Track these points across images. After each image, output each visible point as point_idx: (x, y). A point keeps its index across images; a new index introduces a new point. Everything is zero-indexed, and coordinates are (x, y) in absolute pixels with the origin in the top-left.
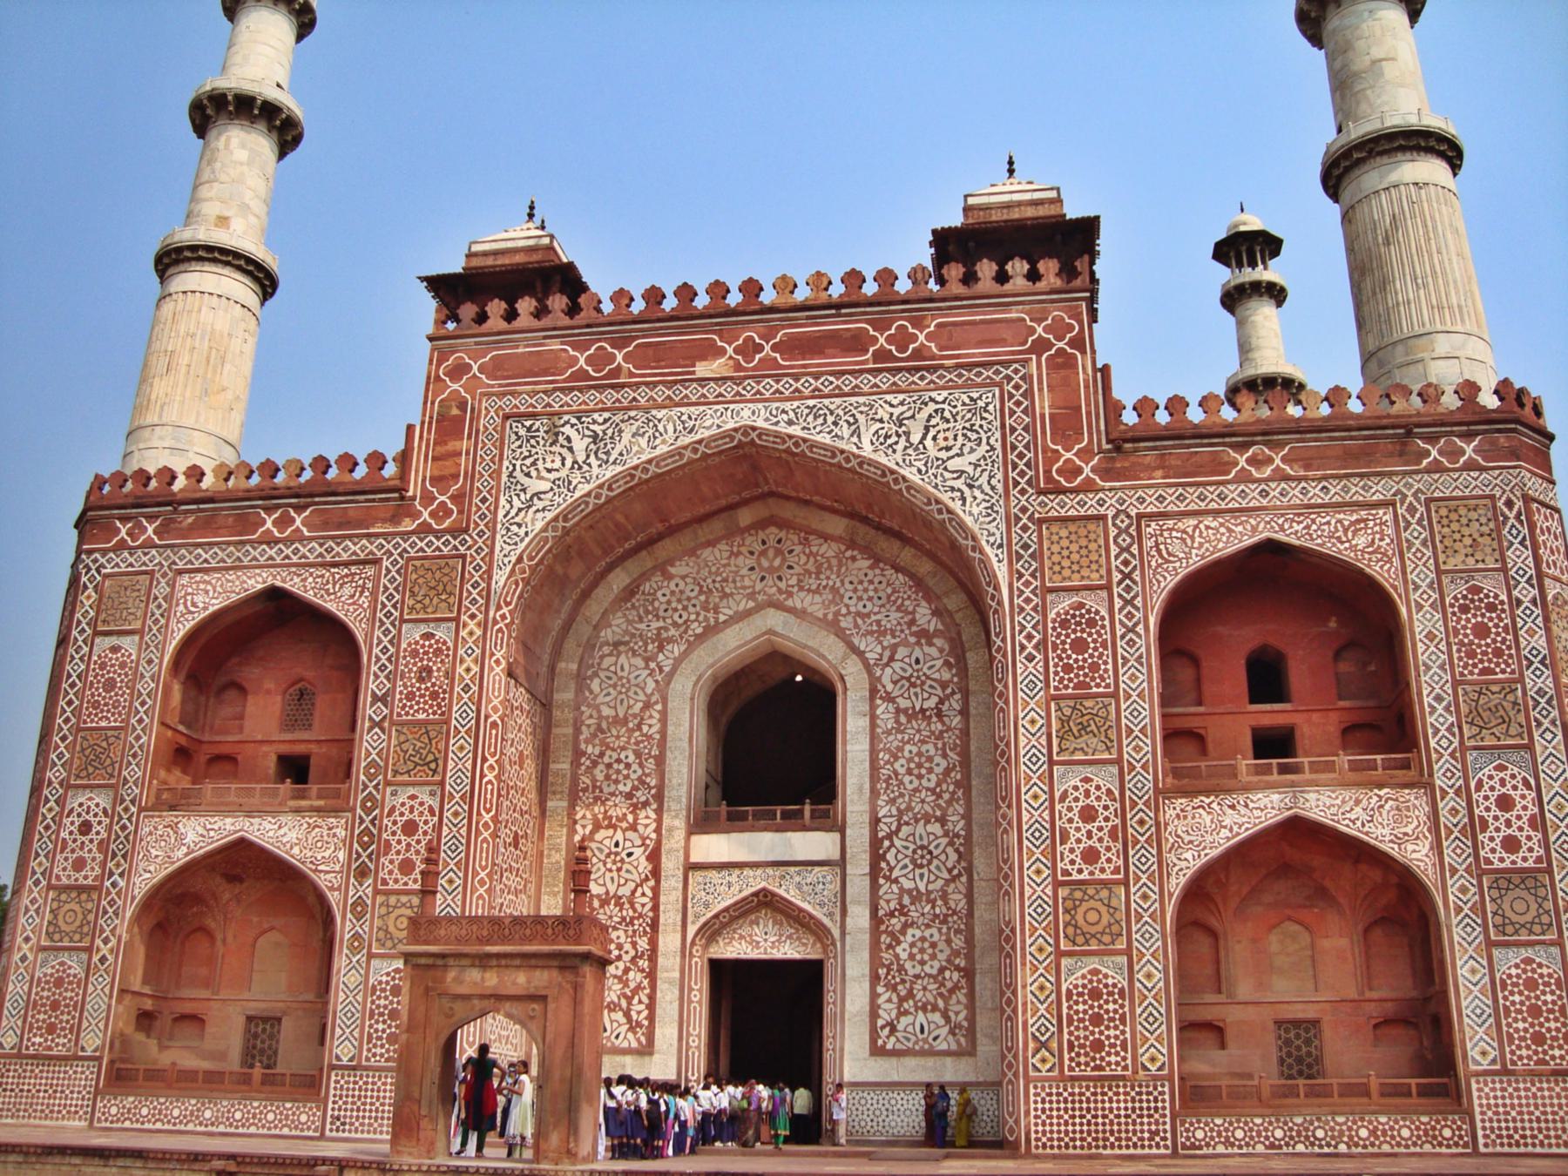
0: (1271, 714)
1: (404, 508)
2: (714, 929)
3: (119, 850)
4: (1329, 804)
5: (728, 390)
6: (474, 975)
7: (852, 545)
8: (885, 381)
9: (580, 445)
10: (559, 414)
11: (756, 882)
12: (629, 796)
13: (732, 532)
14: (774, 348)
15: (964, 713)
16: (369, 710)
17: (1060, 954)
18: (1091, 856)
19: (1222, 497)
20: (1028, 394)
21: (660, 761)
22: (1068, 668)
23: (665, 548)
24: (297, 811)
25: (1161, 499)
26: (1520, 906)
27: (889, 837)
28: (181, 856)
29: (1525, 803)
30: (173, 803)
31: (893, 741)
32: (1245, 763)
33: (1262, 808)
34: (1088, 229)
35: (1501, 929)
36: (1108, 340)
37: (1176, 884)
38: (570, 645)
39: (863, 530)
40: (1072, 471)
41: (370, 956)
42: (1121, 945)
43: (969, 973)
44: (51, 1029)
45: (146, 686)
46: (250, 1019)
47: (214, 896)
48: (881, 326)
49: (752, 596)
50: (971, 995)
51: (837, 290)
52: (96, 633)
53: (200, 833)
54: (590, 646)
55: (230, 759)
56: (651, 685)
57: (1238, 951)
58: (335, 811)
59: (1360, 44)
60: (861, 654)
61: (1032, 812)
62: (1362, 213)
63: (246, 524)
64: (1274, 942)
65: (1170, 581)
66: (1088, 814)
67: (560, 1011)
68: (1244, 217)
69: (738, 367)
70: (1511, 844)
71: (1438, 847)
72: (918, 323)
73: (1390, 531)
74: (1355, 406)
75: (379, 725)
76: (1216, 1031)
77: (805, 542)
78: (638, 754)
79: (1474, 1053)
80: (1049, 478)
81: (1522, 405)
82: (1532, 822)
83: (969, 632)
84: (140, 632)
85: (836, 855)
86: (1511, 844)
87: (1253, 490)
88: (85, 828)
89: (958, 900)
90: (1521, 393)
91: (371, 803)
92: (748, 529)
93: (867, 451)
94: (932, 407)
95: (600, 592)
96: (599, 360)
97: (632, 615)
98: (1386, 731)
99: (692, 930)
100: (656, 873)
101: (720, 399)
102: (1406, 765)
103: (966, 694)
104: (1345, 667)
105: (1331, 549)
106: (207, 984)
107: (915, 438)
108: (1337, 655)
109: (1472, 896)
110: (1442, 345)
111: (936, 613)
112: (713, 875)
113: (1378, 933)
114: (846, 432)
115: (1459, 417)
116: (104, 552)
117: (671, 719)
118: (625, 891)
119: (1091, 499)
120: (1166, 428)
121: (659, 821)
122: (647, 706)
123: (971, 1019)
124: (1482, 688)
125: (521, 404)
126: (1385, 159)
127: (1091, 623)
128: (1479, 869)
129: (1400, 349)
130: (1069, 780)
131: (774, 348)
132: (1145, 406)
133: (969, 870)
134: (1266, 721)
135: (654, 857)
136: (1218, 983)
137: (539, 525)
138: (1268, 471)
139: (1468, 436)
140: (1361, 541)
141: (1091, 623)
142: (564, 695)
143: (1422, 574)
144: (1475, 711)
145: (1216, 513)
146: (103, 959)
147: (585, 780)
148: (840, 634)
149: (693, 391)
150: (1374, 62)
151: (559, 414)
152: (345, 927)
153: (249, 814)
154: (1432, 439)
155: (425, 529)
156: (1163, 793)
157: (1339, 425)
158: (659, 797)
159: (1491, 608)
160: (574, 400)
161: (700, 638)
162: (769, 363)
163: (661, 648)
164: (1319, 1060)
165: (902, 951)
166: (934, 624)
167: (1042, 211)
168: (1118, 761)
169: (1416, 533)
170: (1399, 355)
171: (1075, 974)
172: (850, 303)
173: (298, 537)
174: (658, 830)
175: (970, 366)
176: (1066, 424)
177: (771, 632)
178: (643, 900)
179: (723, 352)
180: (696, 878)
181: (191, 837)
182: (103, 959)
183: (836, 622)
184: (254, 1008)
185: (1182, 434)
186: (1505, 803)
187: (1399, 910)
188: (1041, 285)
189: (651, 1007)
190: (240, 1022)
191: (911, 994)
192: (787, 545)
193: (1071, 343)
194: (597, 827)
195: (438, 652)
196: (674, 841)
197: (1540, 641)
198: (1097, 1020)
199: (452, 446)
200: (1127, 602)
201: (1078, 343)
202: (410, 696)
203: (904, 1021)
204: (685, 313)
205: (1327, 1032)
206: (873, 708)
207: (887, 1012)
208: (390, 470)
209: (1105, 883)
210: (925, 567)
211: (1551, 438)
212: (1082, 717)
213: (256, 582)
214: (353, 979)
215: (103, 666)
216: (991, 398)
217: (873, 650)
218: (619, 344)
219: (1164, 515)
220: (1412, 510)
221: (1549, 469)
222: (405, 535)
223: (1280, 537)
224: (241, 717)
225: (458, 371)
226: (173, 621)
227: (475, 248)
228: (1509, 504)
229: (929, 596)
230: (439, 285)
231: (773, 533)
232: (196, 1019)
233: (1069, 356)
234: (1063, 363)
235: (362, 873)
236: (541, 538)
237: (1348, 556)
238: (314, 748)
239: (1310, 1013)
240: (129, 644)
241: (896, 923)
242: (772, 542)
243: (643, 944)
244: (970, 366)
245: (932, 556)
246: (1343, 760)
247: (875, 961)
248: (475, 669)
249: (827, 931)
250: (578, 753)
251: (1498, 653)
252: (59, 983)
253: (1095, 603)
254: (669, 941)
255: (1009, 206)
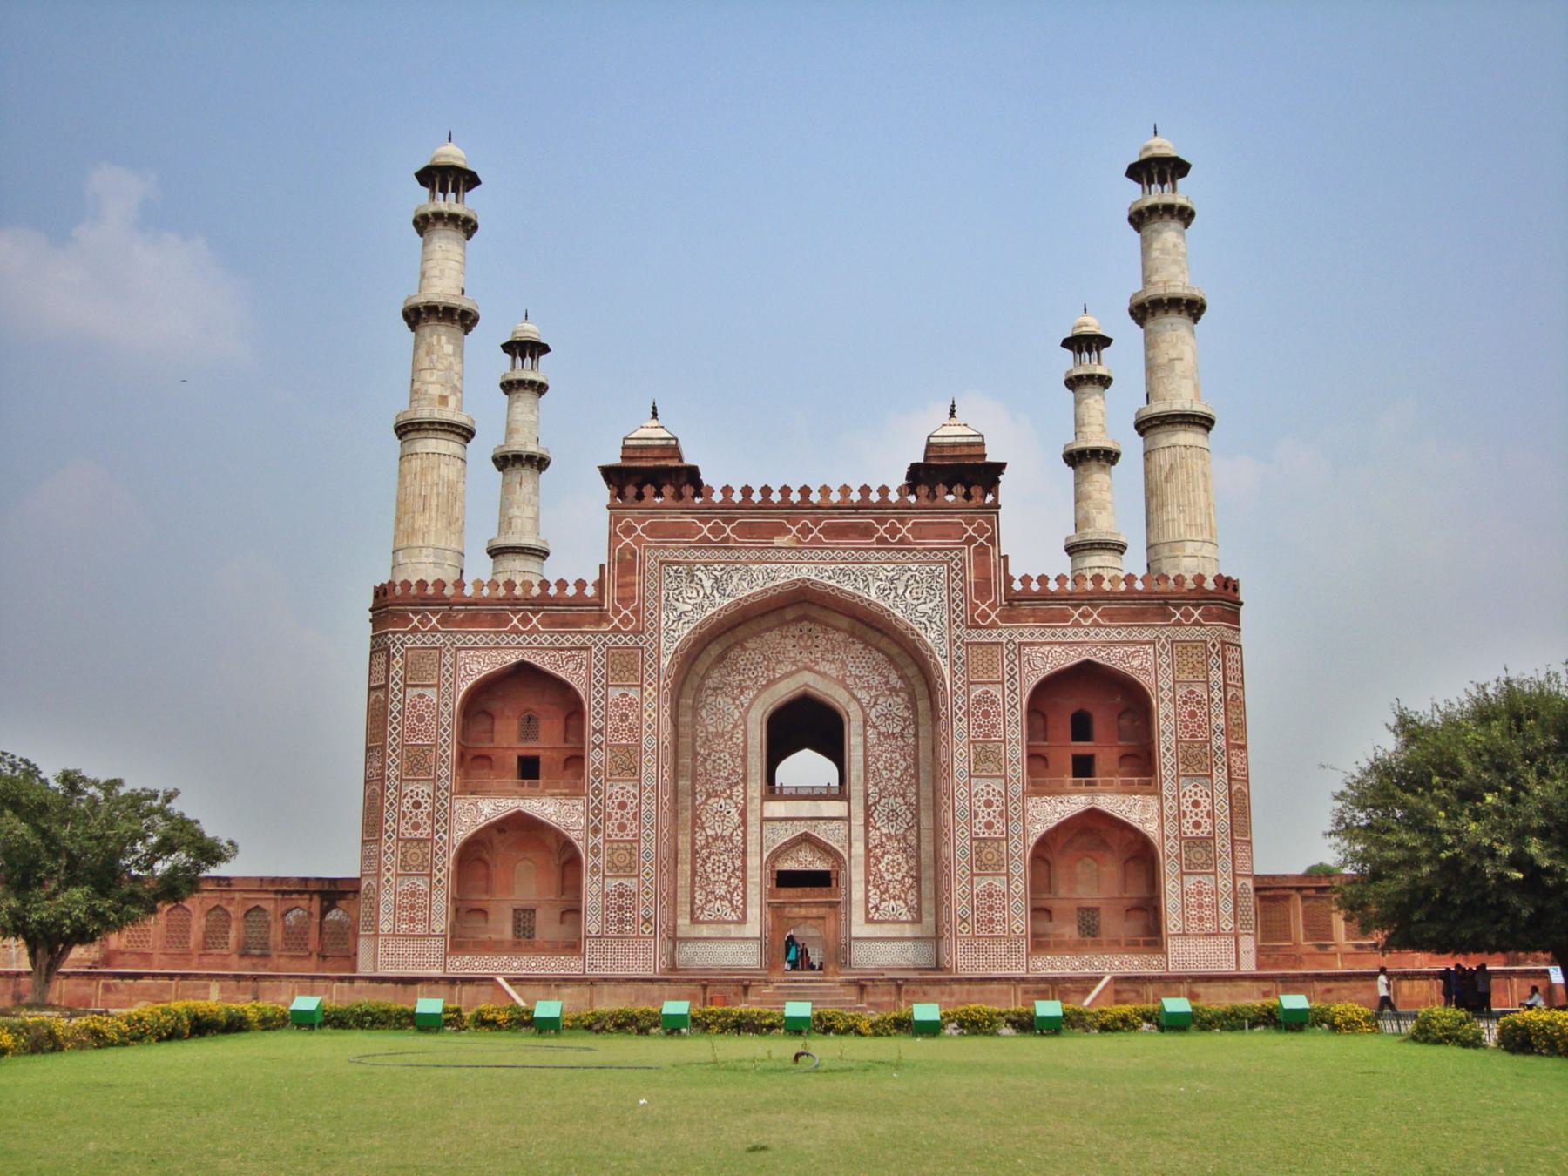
0: (1083, 747)
1: (602, 618)
2: (777, 854)
3: (441, 818)
4: (1111, 803)
5: (794, 555)
6: (796, 910)
7: (852, 634)
8: (883, 555)
9: (707, 583)
10: (694, 563)
11: (801, 828)
12: (727, 779)
13: (783, 623)
14: (820, 531)
15: (916, 735)
16: (591, 738)
17: (973, 875)
18: (989, 825)
19: (1064, 635)
20: (963, 569)
21: (744, 759)
22: (980, 726)
23: (741, 632)
24: (553, 795)
25: (1032, 634)
26: (1198, 855)
27: (875, 804)
28: (482, 822)
29: (1206, 804)
30: (468, 789)
31: (877, 751)
32: (1069, 779)
33: (1075, 803)
34: (999, 468)
35: (1188, 867)
36: (1008, 543)
37: (1032, 840)
38: (687, 688)
39: (859, 625)
40: (985, 616)
41: (604, 876)
42: (1004, 871)
43: (917, 880)
44: (412, 920)
45: (446, 719)
46: (515, 910)
47: (491, 842)
48: (881, 521)
49: (794, 663)
50: (919, 891)
51: (855, 497)
52: (407, 686)
53: (491, 808)
54: (699, 689)
55: (488, 758)
56: (737, 715)
57: (1060, 872)
58: (577, 796)
59: (1164, 346)
60: (858, 700)
61: (961, 802)
62: (1155, 457)
63: (499, 621)
64: (1079, 868)
65: (1034, 681)
66: (988, 804)
67: (831, 923)
68: (1086, 319)
69: (799, 542)
70: (1197, 825)
71: (1162, 825)
72: (902, 521)
73: (1151, 658)
74: (1139, 586)
75: (599, 746)
76: (1048, 912)
77: (825, 632)
78: (731, 755)
79: (1170, 925)
80: (973, 620)
81: (1226, 587)
82: (1208, 814)
83: (920, 690)
84: (438, 686)
85: (845, 814)
86: (1197, 825)
87: (1081, 631)
88: (417, 805)
89: (912, 840)
90: (1228, 579)
91: (597, 792)
92: (788, 623)
93: (873, 597)
94: (909, 573)
95: (704, 656)
96: (716, 530)
97: (724, 671)
98: (1141, 763)
99: (765, 856)
100: (744, 823)
101: (789, 561)
102: (1149, 783)
103: (917, 724)
104: (1124, 722)
105: (1120, 666)
106: (487, 892)
107: (900, 592)
108: (1120, 716)
109: (1176, 849)
110: (1190, 548)
111: (900, 677)
112: (777, 824)
113: (1131, 864)
114: (861, 586)
115: (1193, 595)
116: (405, 634)
117: (750, 735)
118: (726, 833)
119: (995, 633)
120: (1037, 593)
121: (745, 793)
122: (735, 726)
123: (919, 903)
124: (1190, 745)
125: (669, 555)
126: (1169, 428)
127: (993, 702)
128: (1181, 836)
129: (1166, 548)
130: (979, 786)
131: (820, 531)
132: (1026, 580)
133: (918, 824)
134: (1080, 751)
135: (743, 814)
136: (1049, 887)
137: (686, 631)
138: (1090, 621)
139: (1196, 606)
140: (1135, 663)
141: (993, 702)
142: (686, 719)
143: (1165, 682)
144: (1186, 757)
145: (1061, 644)
146: (439, 881)
147: (700, 769)
148: (846, 687)
149: (773, 555)
150: (1171, 360)
151: (694, 563)
152: (587, 860)
153: (523, 797)
154: (1177, 607)
155: (616, 630)
156: (1027, 794)
157: (1130, 595)
158: (745, 780)
159: (1199, 702)
160: (702, 555)
161: (765, 687)
162: (816, 540)
163: (742, 692)
164: (1098, 927)
165: (882, 867)
166: (899, 684)
167: (974, 451)
168: (1005, 777)
169: (1164, 660)
170: (1165, 551)
171: (981, 885)
172: (864, 505)
173: (534, 630)
174: (745, 799)
175: (931, 550)
176: (983, 588)
177: (806, 685)
178: (738, 838)
179: (789, 531)
180: (767, 826)
181: (487, 811)
182: (439, 881)
183: (844, 681)
184: (518, 904)
185: (1045, 596)
186: (1196, 804)
187: (1141, 854)
188: (972, 502)
189: (744, 897)
190: (510, 913)
191: (887, 890)
192: (813, 634)
193: (988, 540)
194: (709, 796)
195: (631, 705)
196: (754, 805)
197: (1221, 721)
198: (991, 908)
199: (628, 579)
200: (1013, 691)
201: (991, 540)
202: (616, 730)
203: (884, 905)
204: (766, 503)
205: (1103, 913)
206: (865, 731)
207: (874, 900)
208: (590, 591)
209: (996, 839)
210: (894, 650)
211: (1241, 604)
212: (986, 755)
213: (511, 658)
214: (595, 889)
215: (414, 706)
216: (942, 570)
217: (865, 697)
218: (729, 521)
219: (1032, 644)
220: (1163, 647)
221: (1237, 622)
222: (605, 633)
223: (1094, 659)
224: (492, 731)
225: (628, 530)
226: (459, 681)
227: (629, 443)
228: (1214, 646)
229: (896, 668)
230: (609, 473)
231: (806, 625)
232: (483, 912)
233: (986, 543)
234: (982, 552)
235: (596, 831)
236: (687, 640)
237: (1128, 671)
238: (541, 752)
239: (1095, 904)
240: (431, 693)
241: (879, 852)
242: (805, 630)
243: (738, 863)
244: (931, 550)
245: (899, 644)
246: (1117, 780)
247: (867, 873)
248: (654, 715)
249: (840, 856)
250: (696, 754)
251: (1200, 726)
252: (413, 894)
253: (995, 691)
254: (753, 862)
255: (954, 445)
